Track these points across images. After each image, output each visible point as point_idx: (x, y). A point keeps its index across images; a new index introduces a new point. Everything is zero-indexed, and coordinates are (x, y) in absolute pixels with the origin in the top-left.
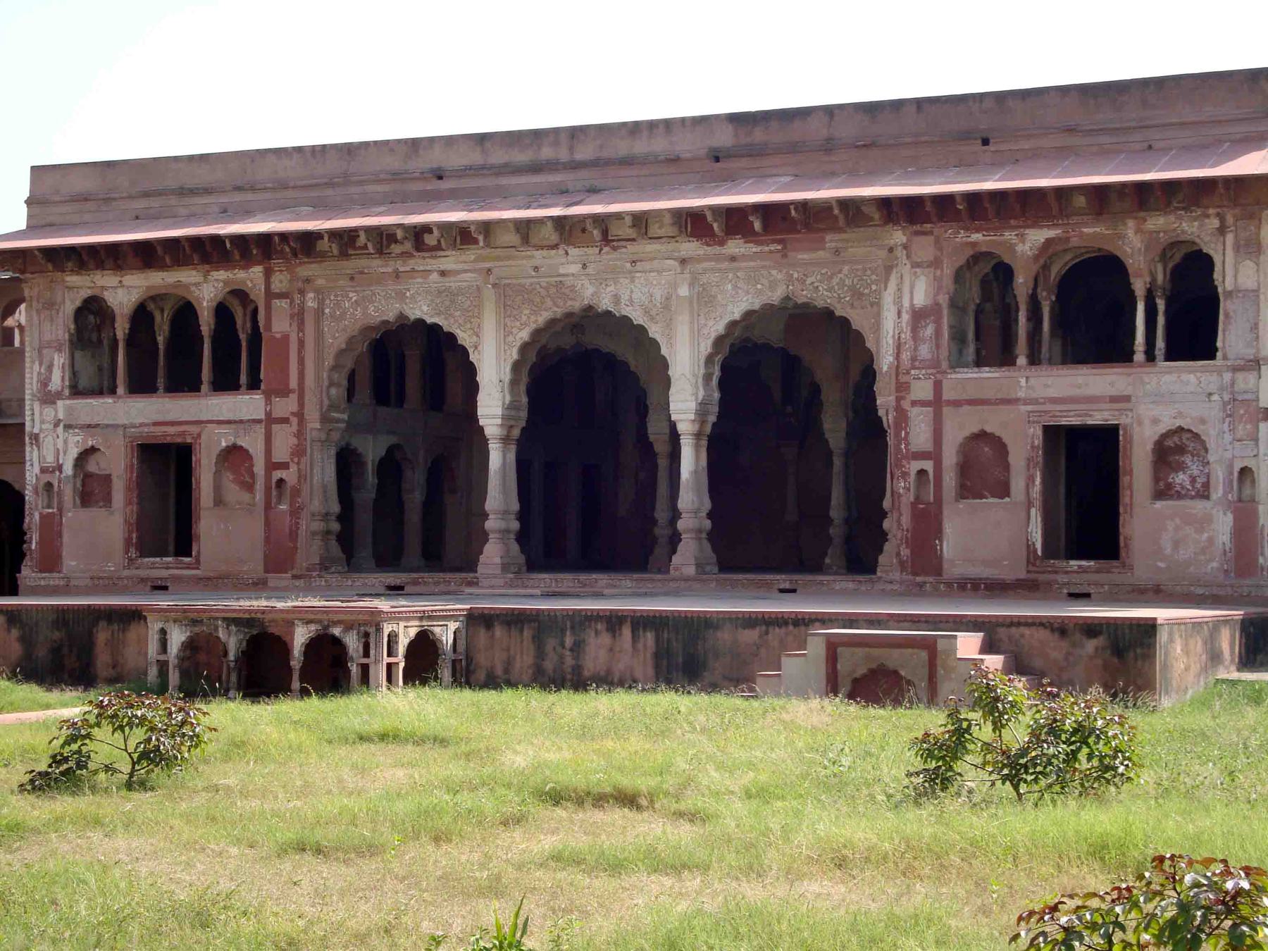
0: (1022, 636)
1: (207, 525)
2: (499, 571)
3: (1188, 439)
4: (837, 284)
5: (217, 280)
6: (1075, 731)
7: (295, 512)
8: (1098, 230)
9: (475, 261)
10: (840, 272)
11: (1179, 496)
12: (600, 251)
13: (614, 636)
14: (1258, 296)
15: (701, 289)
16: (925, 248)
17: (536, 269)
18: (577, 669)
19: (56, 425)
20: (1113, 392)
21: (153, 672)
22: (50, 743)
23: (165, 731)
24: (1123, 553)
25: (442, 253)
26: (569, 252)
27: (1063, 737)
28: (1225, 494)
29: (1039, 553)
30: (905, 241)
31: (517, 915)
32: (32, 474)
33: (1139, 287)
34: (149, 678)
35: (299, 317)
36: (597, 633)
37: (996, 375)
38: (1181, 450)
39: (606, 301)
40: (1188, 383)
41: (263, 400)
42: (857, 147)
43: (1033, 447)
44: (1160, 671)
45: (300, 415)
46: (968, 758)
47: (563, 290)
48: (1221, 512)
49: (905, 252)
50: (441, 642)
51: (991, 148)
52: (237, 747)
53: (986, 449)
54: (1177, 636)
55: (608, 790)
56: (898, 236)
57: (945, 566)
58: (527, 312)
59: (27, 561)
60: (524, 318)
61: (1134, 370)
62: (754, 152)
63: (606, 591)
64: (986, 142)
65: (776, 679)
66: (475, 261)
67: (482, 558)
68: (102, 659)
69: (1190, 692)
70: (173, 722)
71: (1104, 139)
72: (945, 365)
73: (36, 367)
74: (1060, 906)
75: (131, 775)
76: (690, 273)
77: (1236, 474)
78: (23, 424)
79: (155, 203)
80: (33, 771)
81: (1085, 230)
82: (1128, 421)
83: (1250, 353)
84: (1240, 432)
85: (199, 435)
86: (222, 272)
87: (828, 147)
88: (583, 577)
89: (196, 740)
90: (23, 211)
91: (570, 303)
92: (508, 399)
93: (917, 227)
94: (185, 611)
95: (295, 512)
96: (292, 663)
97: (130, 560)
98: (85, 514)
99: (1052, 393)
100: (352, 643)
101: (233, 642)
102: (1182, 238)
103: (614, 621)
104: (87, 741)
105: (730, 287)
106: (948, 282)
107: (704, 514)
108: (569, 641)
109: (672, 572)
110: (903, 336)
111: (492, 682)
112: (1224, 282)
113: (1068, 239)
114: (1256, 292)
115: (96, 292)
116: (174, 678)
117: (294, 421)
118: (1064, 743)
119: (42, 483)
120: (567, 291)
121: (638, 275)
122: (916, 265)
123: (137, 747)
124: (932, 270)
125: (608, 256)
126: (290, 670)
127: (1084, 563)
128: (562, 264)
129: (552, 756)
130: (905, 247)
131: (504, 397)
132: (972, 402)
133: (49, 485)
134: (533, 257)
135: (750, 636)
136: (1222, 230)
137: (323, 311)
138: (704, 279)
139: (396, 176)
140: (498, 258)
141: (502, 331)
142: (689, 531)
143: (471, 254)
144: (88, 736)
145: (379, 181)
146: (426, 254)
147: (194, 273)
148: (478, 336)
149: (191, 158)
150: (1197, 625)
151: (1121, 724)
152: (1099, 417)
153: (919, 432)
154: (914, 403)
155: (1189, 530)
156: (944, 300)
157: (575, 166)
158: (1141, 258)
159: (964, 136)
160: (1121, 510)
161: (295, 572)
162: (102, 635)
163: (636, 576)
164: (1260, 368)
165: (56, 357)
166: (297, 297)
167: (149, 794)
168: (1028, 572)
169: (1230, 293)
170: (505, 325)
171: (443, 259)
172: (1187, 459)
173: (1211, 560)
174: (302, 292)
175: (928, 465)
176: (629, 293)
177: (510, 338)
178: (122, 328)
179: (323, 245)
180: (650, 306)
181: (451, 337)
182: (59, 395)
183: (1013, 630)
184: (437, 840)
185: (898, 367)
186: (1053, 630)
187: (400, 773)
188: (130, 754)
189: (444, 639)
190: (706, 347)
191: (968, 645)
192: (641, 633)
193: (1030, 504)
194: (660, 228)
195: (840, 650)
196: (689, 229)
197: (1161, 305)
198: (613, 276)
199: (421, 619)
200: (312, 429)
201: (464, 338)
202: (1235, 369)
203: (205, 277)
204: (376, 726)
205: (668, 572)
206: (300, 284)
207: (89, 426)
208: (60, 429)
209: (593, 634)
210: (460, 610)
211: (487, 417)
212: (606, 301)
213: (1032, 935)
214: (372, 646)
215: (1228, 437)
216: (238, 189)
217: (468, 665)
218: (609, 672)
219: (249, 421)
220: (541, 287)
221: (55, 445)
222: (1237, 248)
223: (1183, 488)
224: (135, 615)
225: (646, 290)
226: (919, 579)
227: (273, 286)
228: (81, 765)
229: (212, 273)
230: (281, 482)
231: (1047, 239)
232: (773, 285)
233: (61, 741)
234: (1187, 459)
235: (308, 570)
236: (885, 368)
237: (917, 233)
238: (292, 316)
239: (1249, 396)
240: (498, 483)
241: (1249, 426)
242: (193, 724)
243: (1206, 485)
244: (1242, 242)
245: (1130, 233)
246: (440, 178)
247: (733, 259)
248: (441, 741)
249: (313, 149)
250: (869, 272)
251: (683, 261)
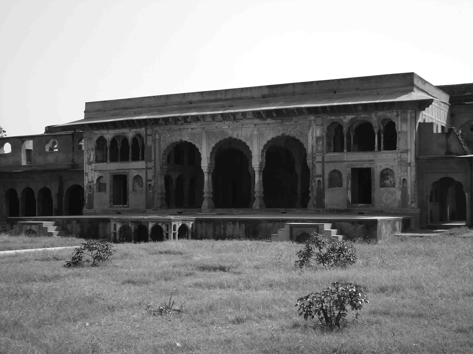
0: (342, 224)
1: (132, 197)
3: (389, 171)
4: (296, 130)
5: (133, 131)
6: (339, 250)
7: (154, 193)
8: (365, 116)
9: (200, 125)
10: (297, 127)
11: (387, 187)
13: (234, 225)
14: (407, 133)
16: (319, 121)
17: (216, 127)
18: (225, 234)
19: (92, 170)
20: (370, 159)
21: (112, 235)
22: (72, 254)
23: (102, 251)
24: (372, 202)
25: (192, 123)
27: (336, 251)
28: (399, 186)
29: (350, 202)
30: (314, 119)
31: (170, 300)
32: (86, 183)
33: (376, 131)
34: (112, 237)
35: (154, 141)
36: (230, 224)
37: (339, 154)
38: (387, 174)
39: (235, 135)
40: (389, 156)
41: (145, 164)
42: (301, 94)
43: (348, 173)
44: (379, 233)
45: (155, 167)
46: (313, 257)
48: (398, 191)
49: (314, 122)
50: (188, 227)
51: (337, 94)
52: (126, 255)
53: (336, 174)
54: (383, 223)
55: (218, 266)
56: (312, 118)
57: (326, 206)
58: (214, 139)
59: (85, 206)
61: (375, 153)
62: (274, 96)
63: (234, 213)
64: (335, 92)
65: (276, 237)
66: (200, 125)
67: (203, 205)
68: (101, 232)
69: (387, 238)
70: (104, 249)
71: (366, 92)
72: (325, 152)
73: (87, 155)
74: (309, 296)
75: (94, 262)
77: (402, 180)
78: (84, 170)
79: (117, 111)
80: (67, 262)
81: (362, 116)
82: (373, 167)
83: (405, 148)
84: (403, 170)
85: (129, 173)
86: (134, 129)
87: (293, 94)
88: (229, 210)
89: (110, 254)
90: (83, 114)
91: (225, 136)
92: (209, 162)
93: (317, 115)
94: (121, 219)
95: (154, 193)
96: (148, 233)
97: (111, 205)
98: (100, 193)
99: (354, 159)
100: (164, 227)
101: (133, 227)
102: (387, 118)
103: (234, 221)
104: (82, 254)
105: (268, 131)
106: (325, 129)
107: (262, 192)
108: (222, 227)
110: (314, 144)
111: (201, 238)
112: (398, 129)
113: (357, 118)
114: (407, 132)
115: (102, 135)
116: (118, 237)
117: (153, 168)
118: (336, 253)
119: (88, 186)
120: (225, 133)
121: (243, 128)
122: (317, 125)
123: (94, 255)
124: (321, 126)
125: (236, 124)
126: (148, 234)
127: (362, 205)
129: (207, 257)
130: (314, 120)
132: (332, 162)
133: (90, 186)
134: (216, 124)
135: (270, 225)
136: (397, 116)
137: (161, 140)
138: (261, 129)
139: (180, 103)
140: (206, 125)
142: (257, 197)
143: (199, 124)
144: (82, 252)
145: (175, 105)
146: (187, 124)
147: (127, 130)
148: (201, 145)
149: (126, 99)
150: (389, 221)
151: (352, 248)
152: (366, 165)
153: (318, 170)
154: (317, 162)
155: (390, 195)
156: (324, 135)
157: (227, 100)
158: (377, 123)
159: (329, 91)
160: (372, 190)
161: (154, 209)
162: (101, 225)
163: (243, 209)
164: (408, 153)
165: (92, 152)
166: (154, 135)
167: (97, 268)
168: (348, 207)
169: (400, 132)
171: (192, 125)
172: (389, 177)
173: (396, 204)
174: (155, 135)
175: (321, 179)
177: (210, 146)
178: (108, 144)
179: (161, 122)
181: (194, 146)
182: (92, 162)
183: (340, 223)
184: (166, 280)
185: (312, 153)
186: (350, 223)
187: (167, 262)
188: (93, 257)
189: (189, 226)
190: (262, 148)
191: (327, 227)
192: (241, 224)
193: (348, 189)
194: (249, 116)
195: (293, 228)
196: (257, 116)
197: (382, 135)
199: (182, 221)
200: (158, 171)
201: (197, 146)
202: (401, 153)
203: (130, 130)
204: (164, 249)
205: (252, 208)
206: (155, 132)
207: (100, 171)
208: (93, 172)
209: (228, 224)
210: (193, 218)
211: (203, 167)
213: (300, 304)
214: (169, 228)
215: (400, 171)
216: (138, 107)
217: (196, 233)
218: (233, 235)
219: (142, 168)
221: (92, 175)
222: (401, 120)
223: (388, 184)
224: (108, 221)
226: (319, 209)
227: (147, 133)
228: (80, 260)
229: (132, 130)
230: (150, 185)
231: (351, 118)
232: (279, 131)
233: (75, 254)
234: (389, 177)
235: (157, 208)
236: (309, 153)
237: (317, 117)
238: (152, 141)
239: (405, 160)
241: (405, 168)
242: (109, 249)
243: (394, 184)
244: (403, 119)
245: (373, 116)
246: (191, 103)
247: (268, 124)
248: (181, 253)
249: (158, 97)
250: (304, 127)
251: (255, 125)
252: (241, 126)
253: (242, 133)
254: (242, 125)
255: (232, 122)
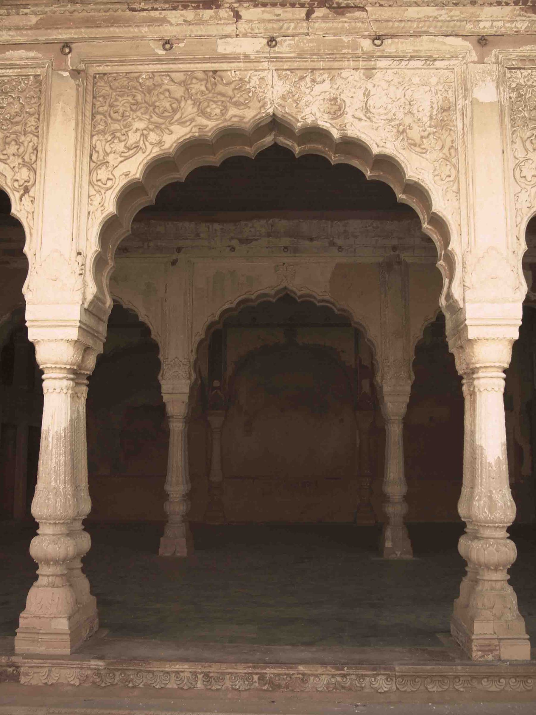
2: (67, 651)
9: (36, 27)
12: (309, 15)
15: (513, 95)
17: (167, 44)
26: (243, 13)
39: (314, 109)
47: (220, 88)
58: (141, 125)
60: (133, 138)
76: (497, 63)
91: (233, 111)
109: (476, 654)
120: (229, 90)
121: (382, 63)
128: (226, 36)
131: (85, 285)
134: (164, 21)
140: (89, 23)
141: (87, 159)
170: (93, 148)
176: (362, 98)
177: (103, 174)
180: (408, 120)
198: (328, 65)
212: (314, 109)
220: (172, 80)
225: (399, 93)
240: (62, 458)
252: (366, 44)
253: (367, 94)
254: (378, 38)
255: (302, 13)
